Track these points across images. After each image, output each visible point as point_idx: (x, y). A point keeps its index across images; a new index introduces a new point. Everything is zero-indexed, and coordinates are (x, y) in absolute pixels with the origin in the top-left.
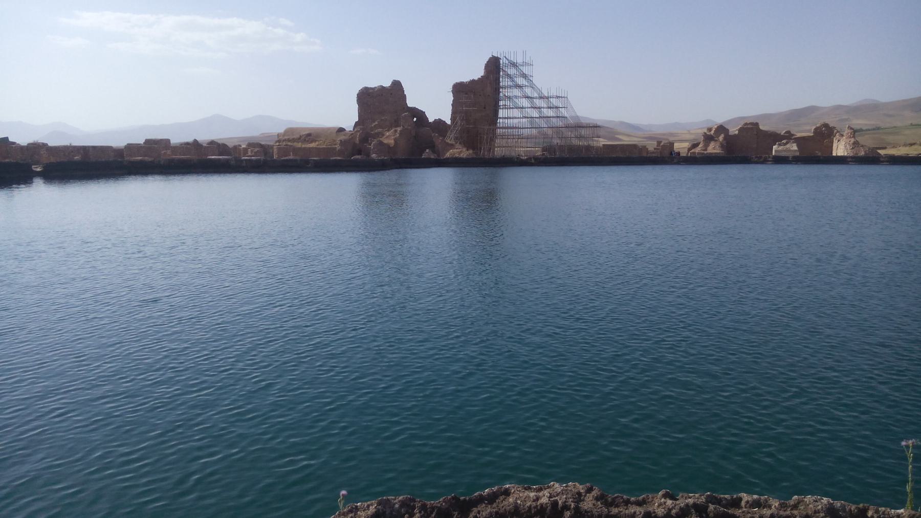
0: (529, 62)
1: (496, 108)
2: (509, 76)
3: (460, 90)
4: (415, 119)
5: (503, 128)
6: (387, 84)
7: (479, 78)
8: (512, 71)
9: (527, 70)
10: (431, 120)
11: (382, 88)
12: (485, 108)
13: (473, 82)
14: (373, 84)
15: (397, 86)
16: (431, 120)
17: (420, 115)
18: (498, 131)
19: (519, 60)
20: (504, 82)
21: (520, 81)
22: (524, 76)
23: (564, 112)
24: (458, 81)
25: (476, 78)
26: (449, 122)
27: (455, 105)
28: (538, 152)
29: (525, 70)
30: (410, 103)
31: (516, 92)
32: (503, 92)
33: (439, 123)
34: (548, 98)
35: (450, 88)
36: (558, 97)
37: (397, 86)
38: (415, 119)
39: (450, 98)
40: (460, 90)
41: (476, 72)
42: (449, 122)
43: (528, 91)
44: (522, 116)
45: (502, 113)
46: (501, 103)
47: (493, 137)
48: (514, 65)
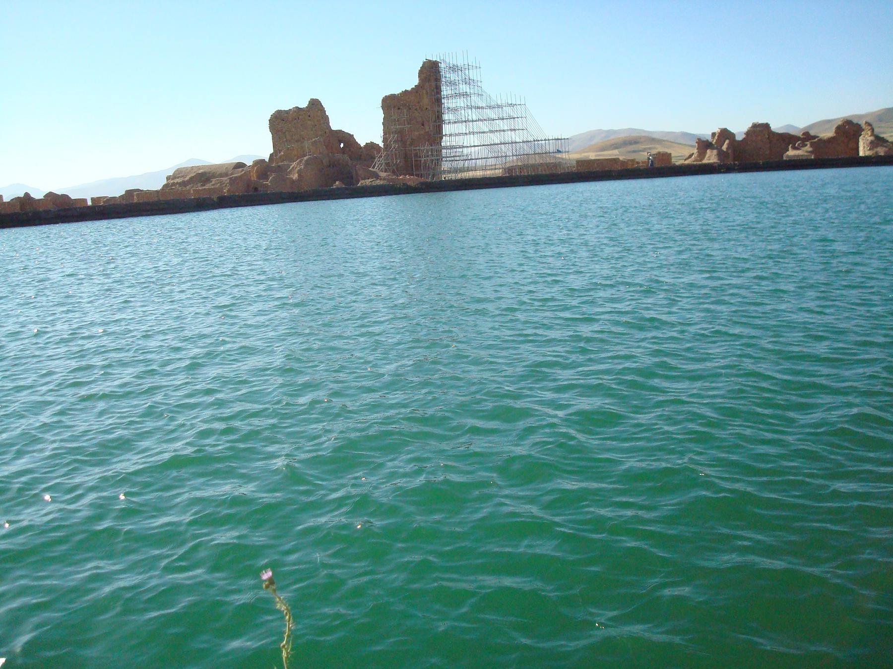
0: (474, 65)
1: (438, 121)
2: (452, 83)
3: (391, 104)
4: (342, 145)
5: (452, 147)
6: (304, 104)
7: (412, 89)
8: (453, 77)
9: (475, 74)
10: (362, 145)
11: (298, 109)
12: (423, 125)
13: (406, 93)
14: (287, 105)
15: (315, 105)
16: (362, 145)
17: (347, 139)
18: (444, 151)
19: (460, 63)
20: (446, 91)
21: (463, 88)
22: (468, 81)
23: (518, 124)
24: (388, 94)
25: (409, 89)
26: (381, 145)
27: (385, 123)
28: (498, 173)
29: (473, 74)
30: (335, 126)
31: (461, 102)
32: (447, 103)
33: (371, 146)
34: (499, 106)
35: (379, 103)
36: (511, 105)
37: (315, 105)
38: (342, 145)
39: (380, 115)
40: (391, 104)
41: (411, 81)
42: (381, 145)
43: (476, 100)
44: (468, 132)
45: (446, 129)
46: (446, 117)
47: (439, 159)
48: (454, 69)
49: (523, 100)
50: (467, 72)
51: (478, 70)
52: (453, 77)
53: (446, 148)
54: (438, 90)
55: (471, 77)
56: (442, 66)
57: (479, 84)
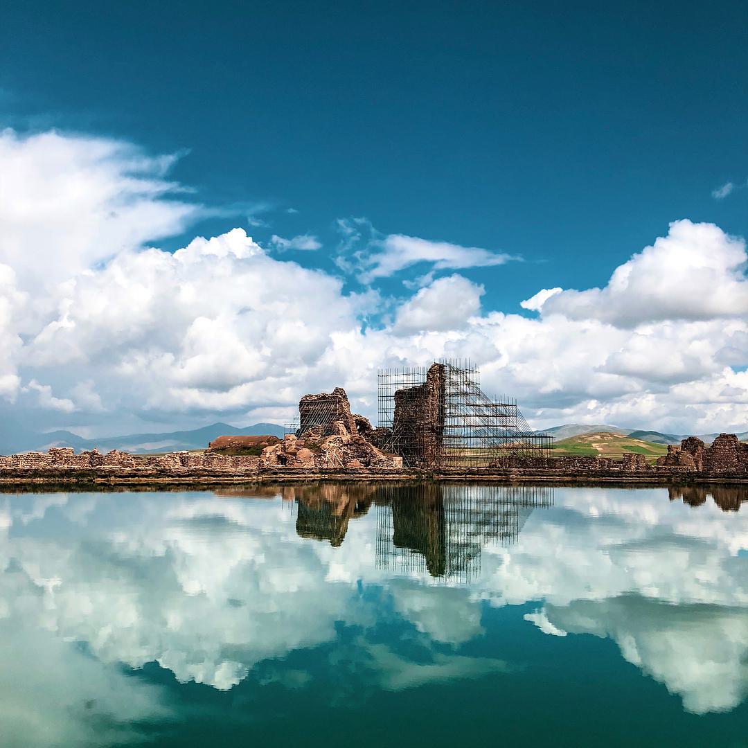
6: (329, 391)
20: (449, 389)
21: (464, 388)
29: (472, 377)
31: (462, 400)
38: (358, 428)
45: (447, 422)
48: (458, 371)
49: (514, 401)
50: (468, 375)
51: (477, 374)
52: (454, 378)
53: (446, 437)
54: (442, 389)
55: (471, 380)
56: (447, 368)
57: (478, 386)
